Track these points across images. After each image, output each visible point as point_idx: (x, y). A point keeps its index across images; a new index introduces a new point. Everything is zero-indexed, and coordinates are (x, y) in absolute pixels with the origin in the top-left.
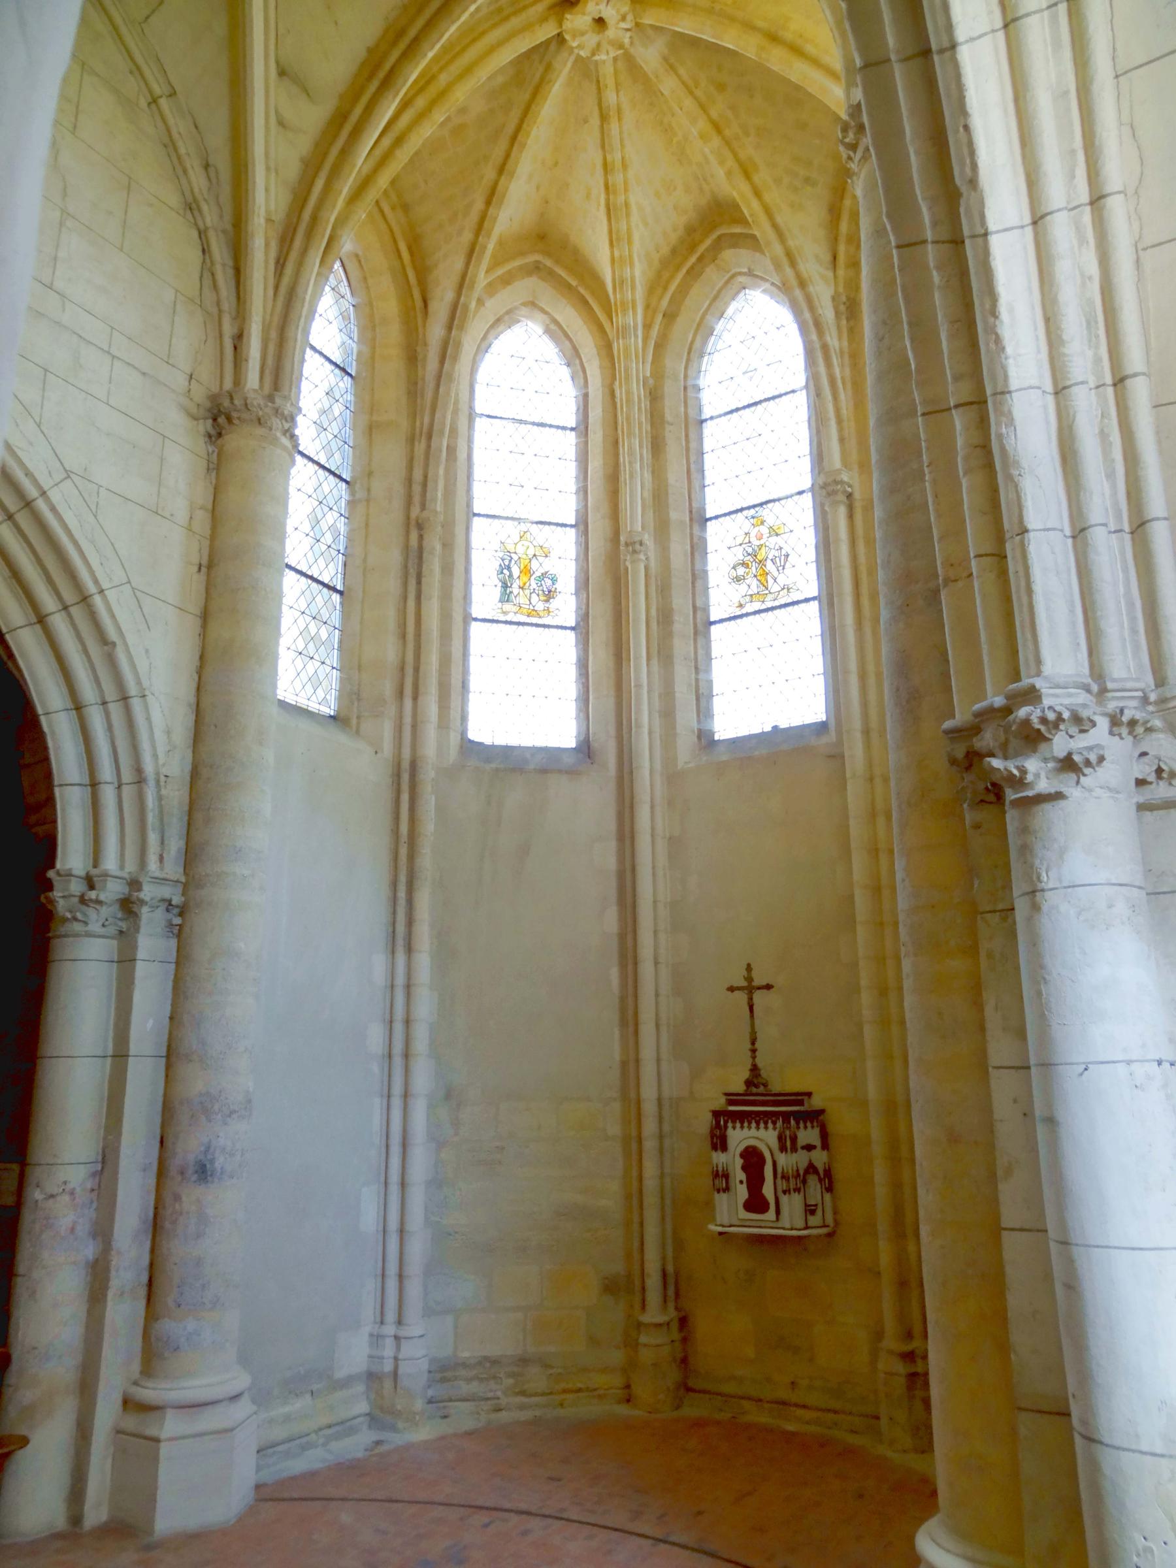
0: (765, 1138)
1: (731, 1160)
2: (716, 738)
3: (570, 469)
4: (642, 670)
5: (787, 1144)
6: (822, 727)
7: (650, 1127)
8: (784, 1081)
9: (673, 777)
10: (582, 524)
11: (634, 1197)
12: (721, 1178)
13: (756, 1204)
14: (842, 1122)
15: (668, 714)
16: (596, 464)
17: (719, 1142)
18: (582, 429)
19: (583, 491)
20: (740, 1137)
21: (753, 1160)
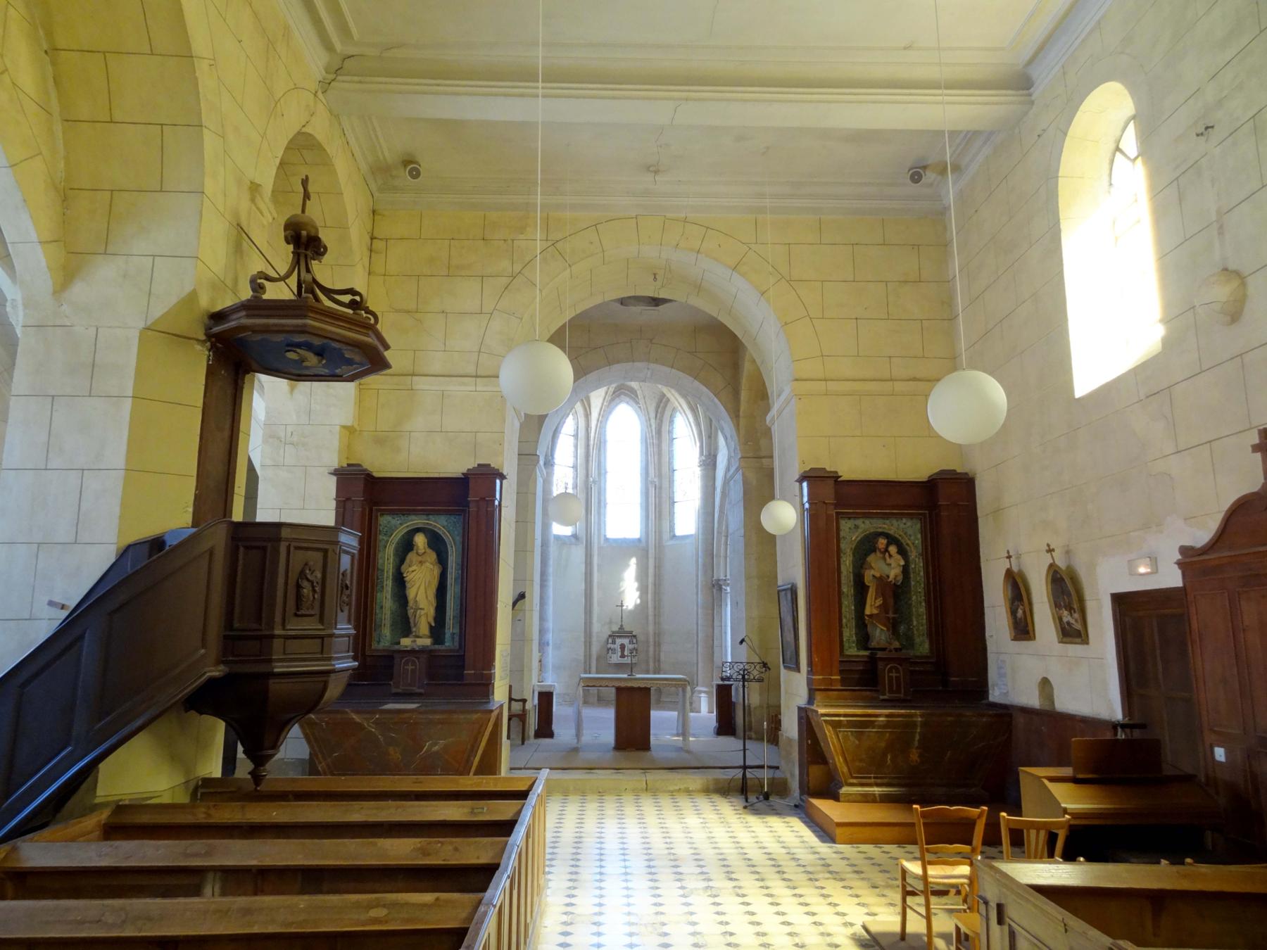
0: (626, 641)
1: (617, 646)
2: (609, 536)
3: (572, 449)
4: (594, 518)
5: (631, 642)
6: (639, 540)
7: (594, 639)
8: (627, 629)
9: (600, 548)
10: (575, 467)
11: (588, 656)
12: (614, 651)
13: (623, 656)
14: (641, 638)
15: (599, 530)
16: (581, 451)
17: (614, 642)
18: (576, 436)
19: (576, 457)
20: (619, 641)
21: (623, 647)
